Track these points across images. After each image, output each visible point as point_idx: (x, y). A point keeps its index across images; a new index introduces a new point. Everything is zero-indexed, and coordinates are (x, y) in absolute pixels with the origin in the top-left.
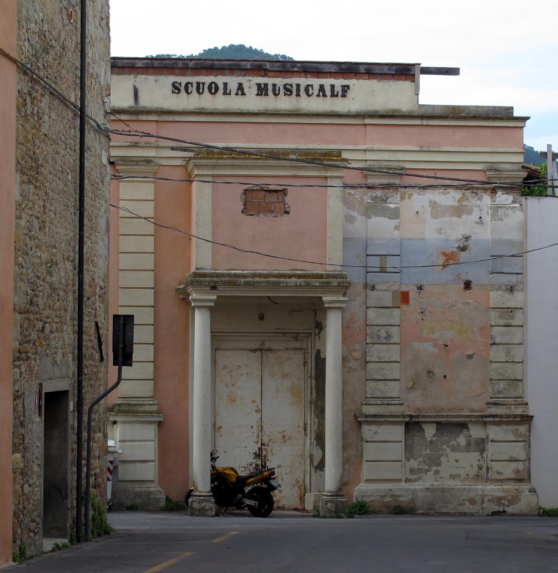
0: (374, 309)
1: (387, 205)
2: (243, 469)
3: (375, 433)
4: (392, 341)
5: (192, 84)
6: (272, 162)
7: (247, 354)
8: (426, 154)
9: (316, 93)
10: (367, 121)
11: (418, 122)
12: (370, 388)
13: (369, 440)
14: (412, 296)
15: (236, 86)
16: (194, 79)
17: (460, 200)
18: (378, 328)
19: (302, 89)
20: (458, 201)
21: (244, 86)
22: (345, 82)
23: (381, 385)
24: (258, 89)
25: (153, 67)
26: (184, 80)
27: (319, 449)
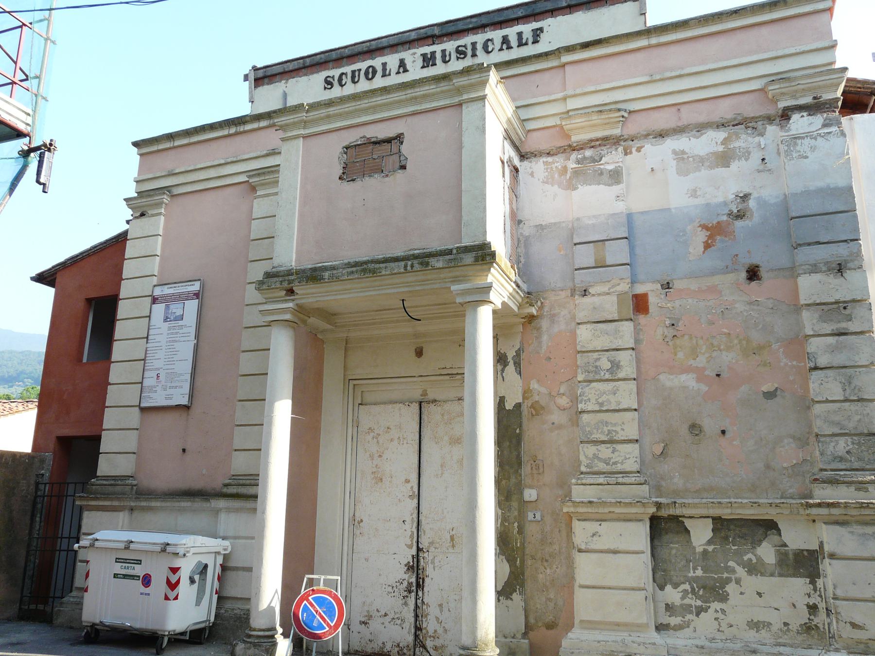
0: (588, 326)
1: (602, 167)
2: (390, 589)
3: (594, 535)
4: (621, 375)
5: (346, 74)
6: (379, 98)
7: (400, 409)
8: (660, 83)
9: (498, 46)
10: (566, 58)
11: (643, 42)
12: (586, 457)
13: (583, 547)
14: (652, 300)
15: (397, 63)
16: (348, 69)
17: (725, 142)
18: (595, 355)
19: (479, 47)
20: (722, 144)
21: (406, 62)
22: (536, 25)
23: (605, 451)
24: (424, 61)
25: (305, 67)
26: (336, 73)
27: (505, 561)
